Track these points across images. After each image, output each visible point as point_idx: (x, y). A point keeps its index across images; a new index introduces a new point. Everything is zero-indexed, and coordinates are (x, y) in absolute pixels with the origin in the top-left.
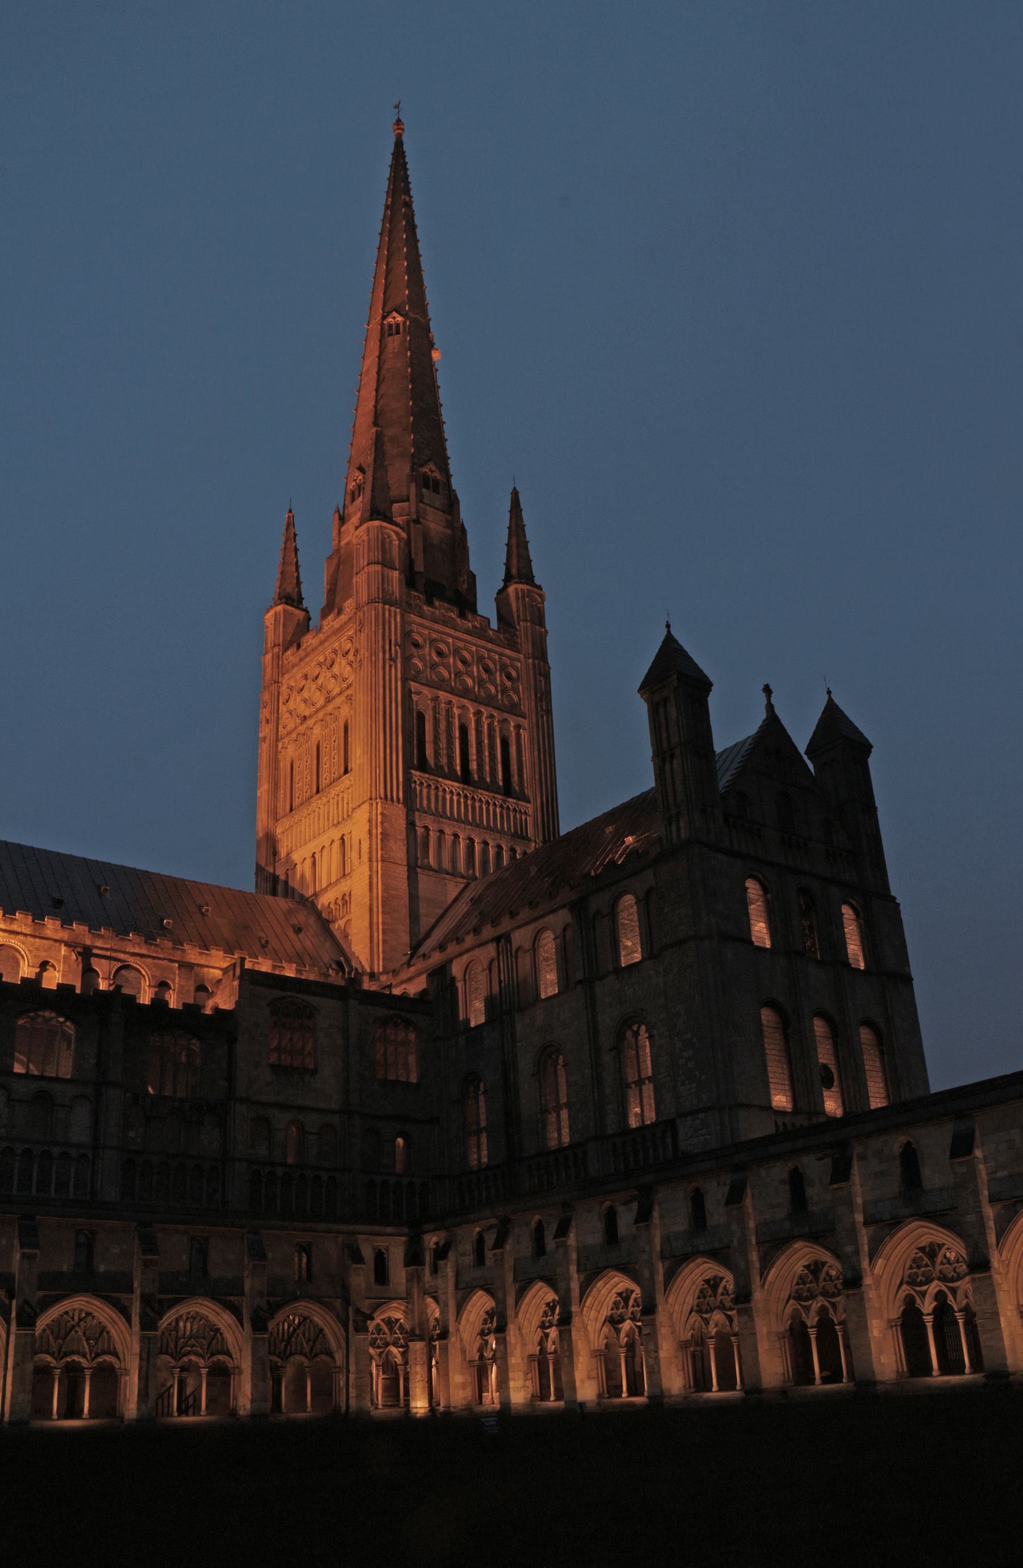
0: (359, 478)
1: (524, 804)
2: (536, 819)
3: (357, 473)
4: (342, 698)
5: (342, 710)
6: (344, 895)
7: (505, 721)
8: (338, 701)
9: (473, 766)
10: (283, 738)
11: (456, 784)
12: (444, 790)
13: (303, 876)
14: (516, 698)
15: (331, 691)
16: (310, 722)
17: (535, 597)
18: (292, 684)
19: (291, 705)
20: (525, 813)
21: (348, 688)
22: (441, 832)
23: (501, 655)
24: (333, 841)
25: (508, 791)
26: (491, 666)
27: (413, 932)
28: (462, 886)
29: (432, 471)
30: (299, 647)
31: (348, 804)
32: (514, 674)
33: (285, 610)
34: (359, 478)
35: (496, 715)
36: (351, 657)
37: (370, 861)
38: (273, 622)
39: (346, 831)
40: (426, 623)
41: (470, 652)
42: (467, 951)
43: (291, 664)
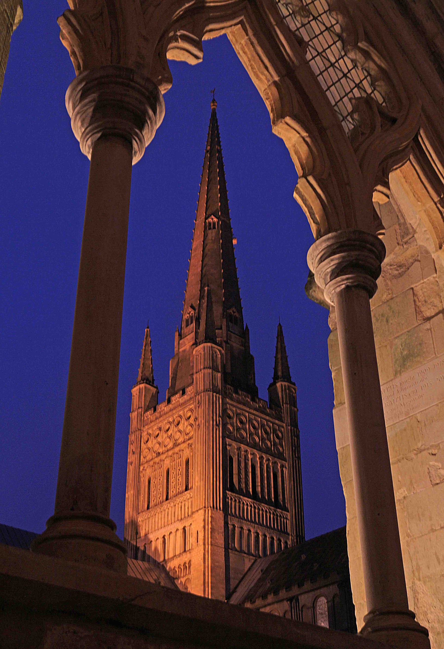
0: (192, 312)
1: (286, 513)
2: (292, 523)
3: (190, 309)
4: (185, 445)
5: (184, 452)
6: (185, 563)
7: (275, 463)
8: (182, 446)
9: (259, 489)
10: (144, 464)
11: (250, 500)
12: (243, 503)
13: (156, 549)
14: (281, 449)
15: (177, 440)
16: (163, 457)
17: (292, 390)
18: (150, 431)
19: (150, 444)
20: (286, 518)
21: (189, 439)
22: (242, 528)
23: (273, 423)
24: (177, 530)
25: (277, 505)
26: (268, 429)
27: (227, 589)
28: (253, 561)
29: (234, 312)
30: (155, 410)
31: (188, 508)
32: (280, 435)
33: (145, 387)
34: (192, 312)
35: (271, 459)
36: (192, 420)
37: (204, 544)
38: (138, 394)
39: (187, 524)
40: (235, 404)
41: (257, 421)
42: (269, 604)
43: (149, 420)
